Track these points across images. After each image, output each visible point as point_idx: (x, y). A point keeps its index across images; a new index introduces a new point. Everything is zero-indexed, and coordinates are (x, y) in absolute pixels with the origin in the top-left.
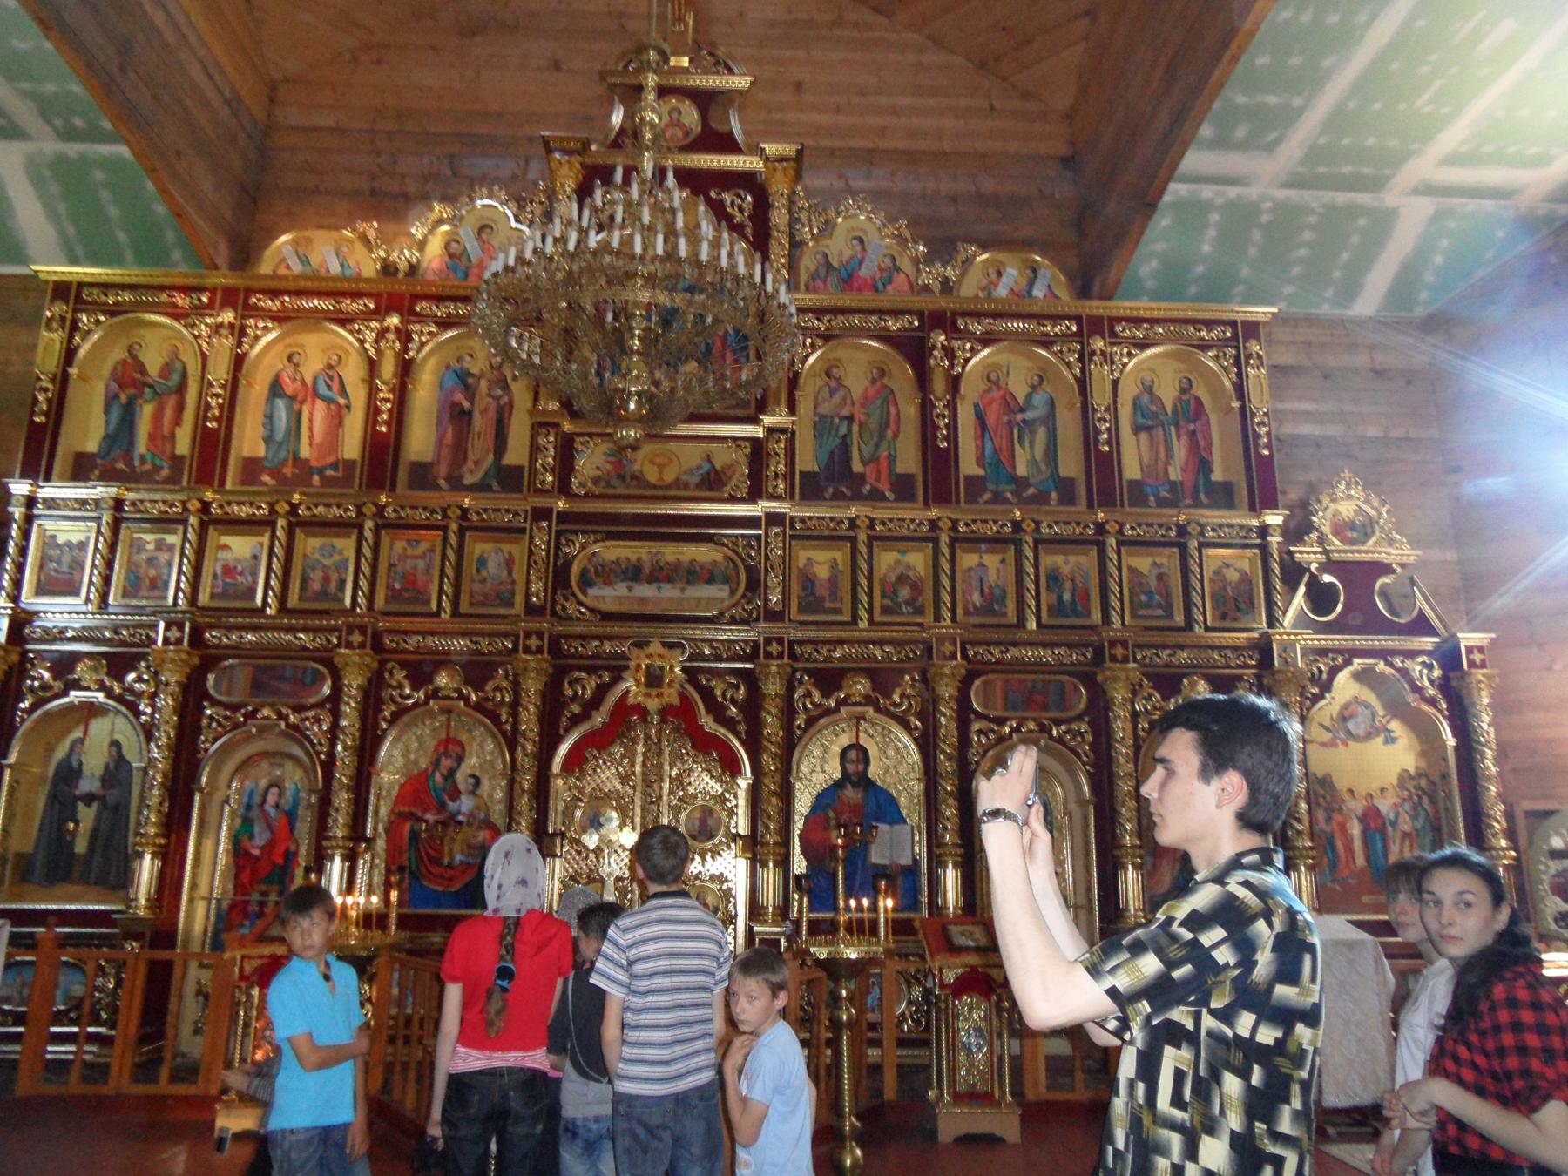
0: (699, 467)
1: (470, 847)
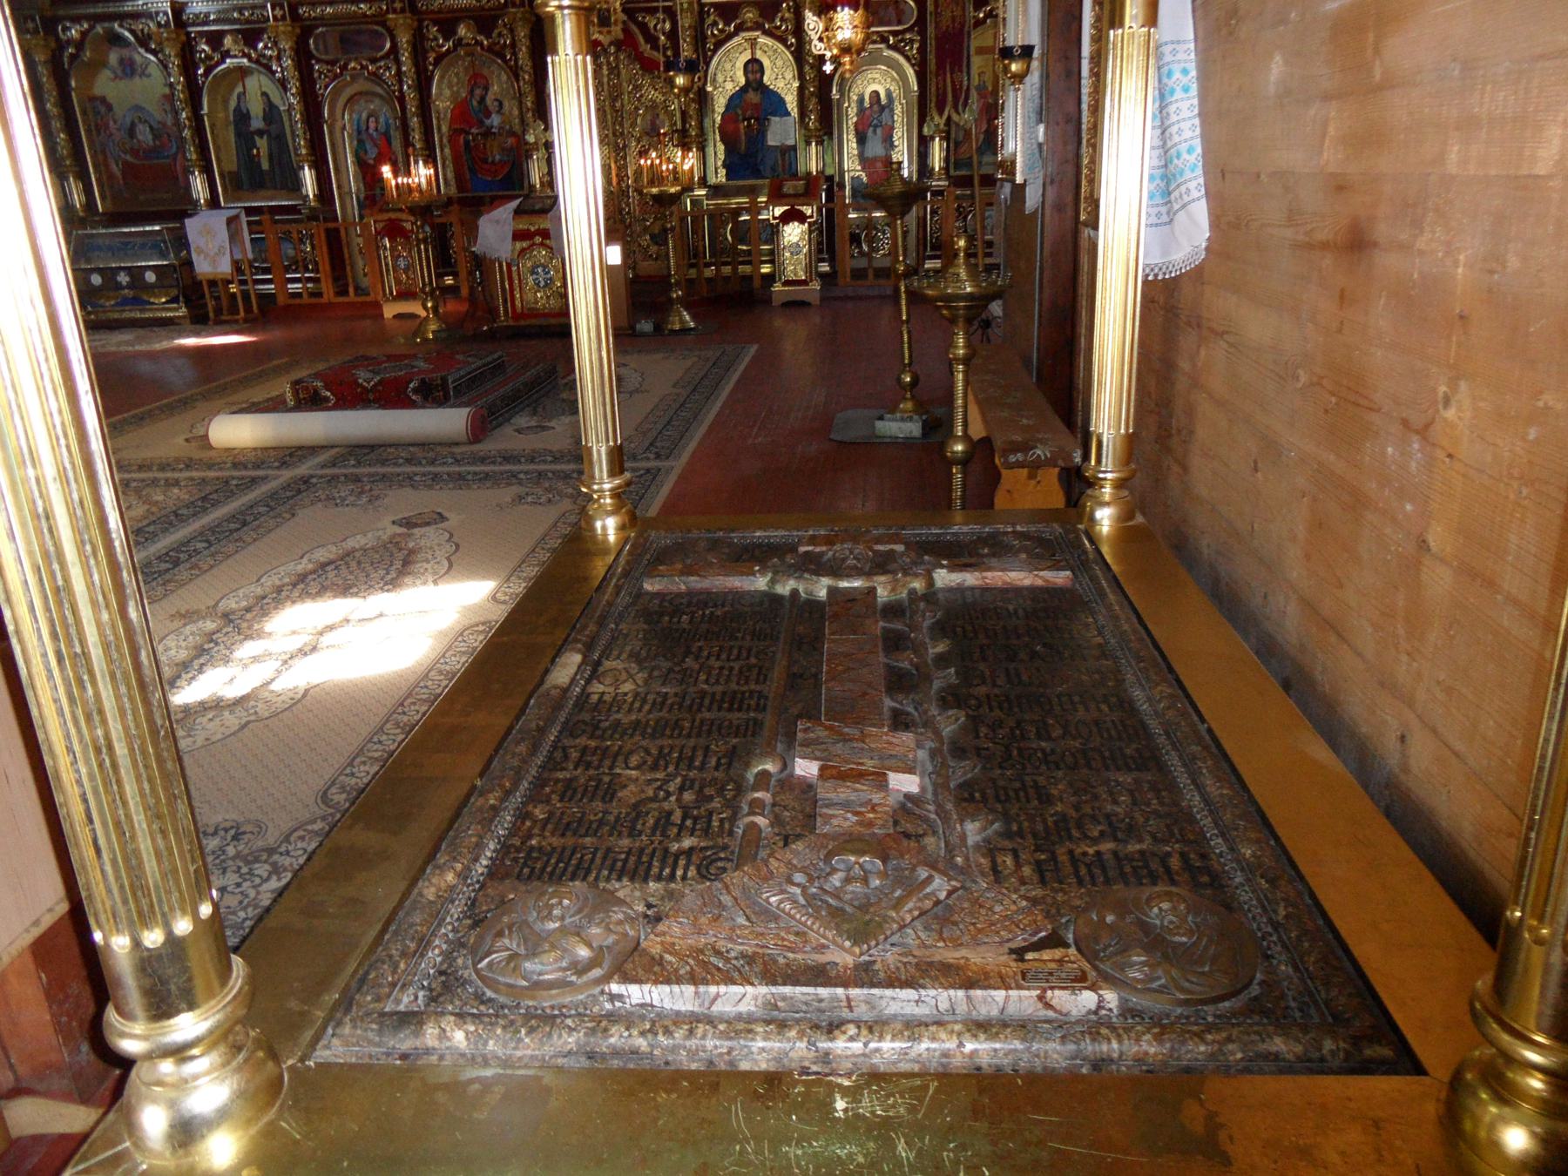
1: (503, 149)
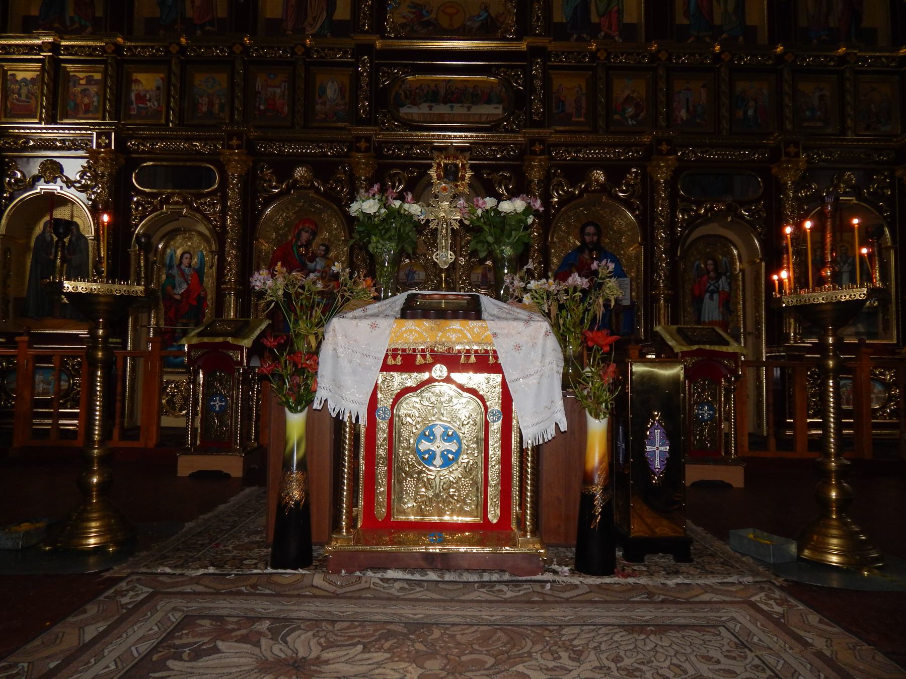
0: (479, 16)
